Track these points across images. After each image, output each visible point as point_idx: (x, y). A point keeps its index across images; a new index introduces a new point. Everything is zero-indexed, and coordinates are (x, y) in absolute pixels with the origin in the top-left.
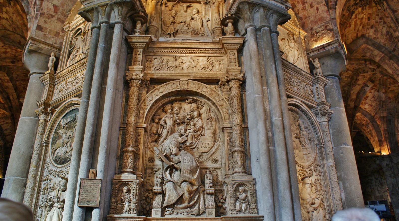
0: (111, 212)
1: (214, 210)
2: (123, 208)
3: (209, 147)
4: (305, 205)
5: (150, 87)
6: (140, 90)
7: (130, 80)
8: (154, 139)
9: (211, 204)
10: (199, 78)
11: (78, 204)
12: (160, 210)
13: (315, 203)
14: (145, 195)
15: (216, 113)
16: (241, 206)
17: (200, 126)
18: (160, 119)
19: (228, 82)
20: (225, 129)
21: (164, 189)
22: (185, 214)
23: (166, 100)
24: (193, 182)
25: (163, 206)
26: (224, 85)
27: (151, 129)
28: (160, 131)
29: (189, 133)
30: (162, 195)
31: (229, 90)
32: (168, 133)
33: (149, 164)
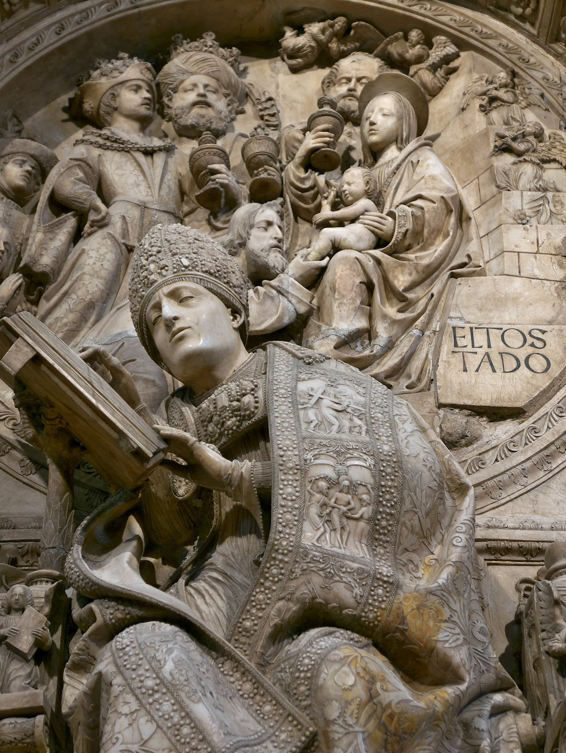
3: (537, 363)
28: (43, 246)
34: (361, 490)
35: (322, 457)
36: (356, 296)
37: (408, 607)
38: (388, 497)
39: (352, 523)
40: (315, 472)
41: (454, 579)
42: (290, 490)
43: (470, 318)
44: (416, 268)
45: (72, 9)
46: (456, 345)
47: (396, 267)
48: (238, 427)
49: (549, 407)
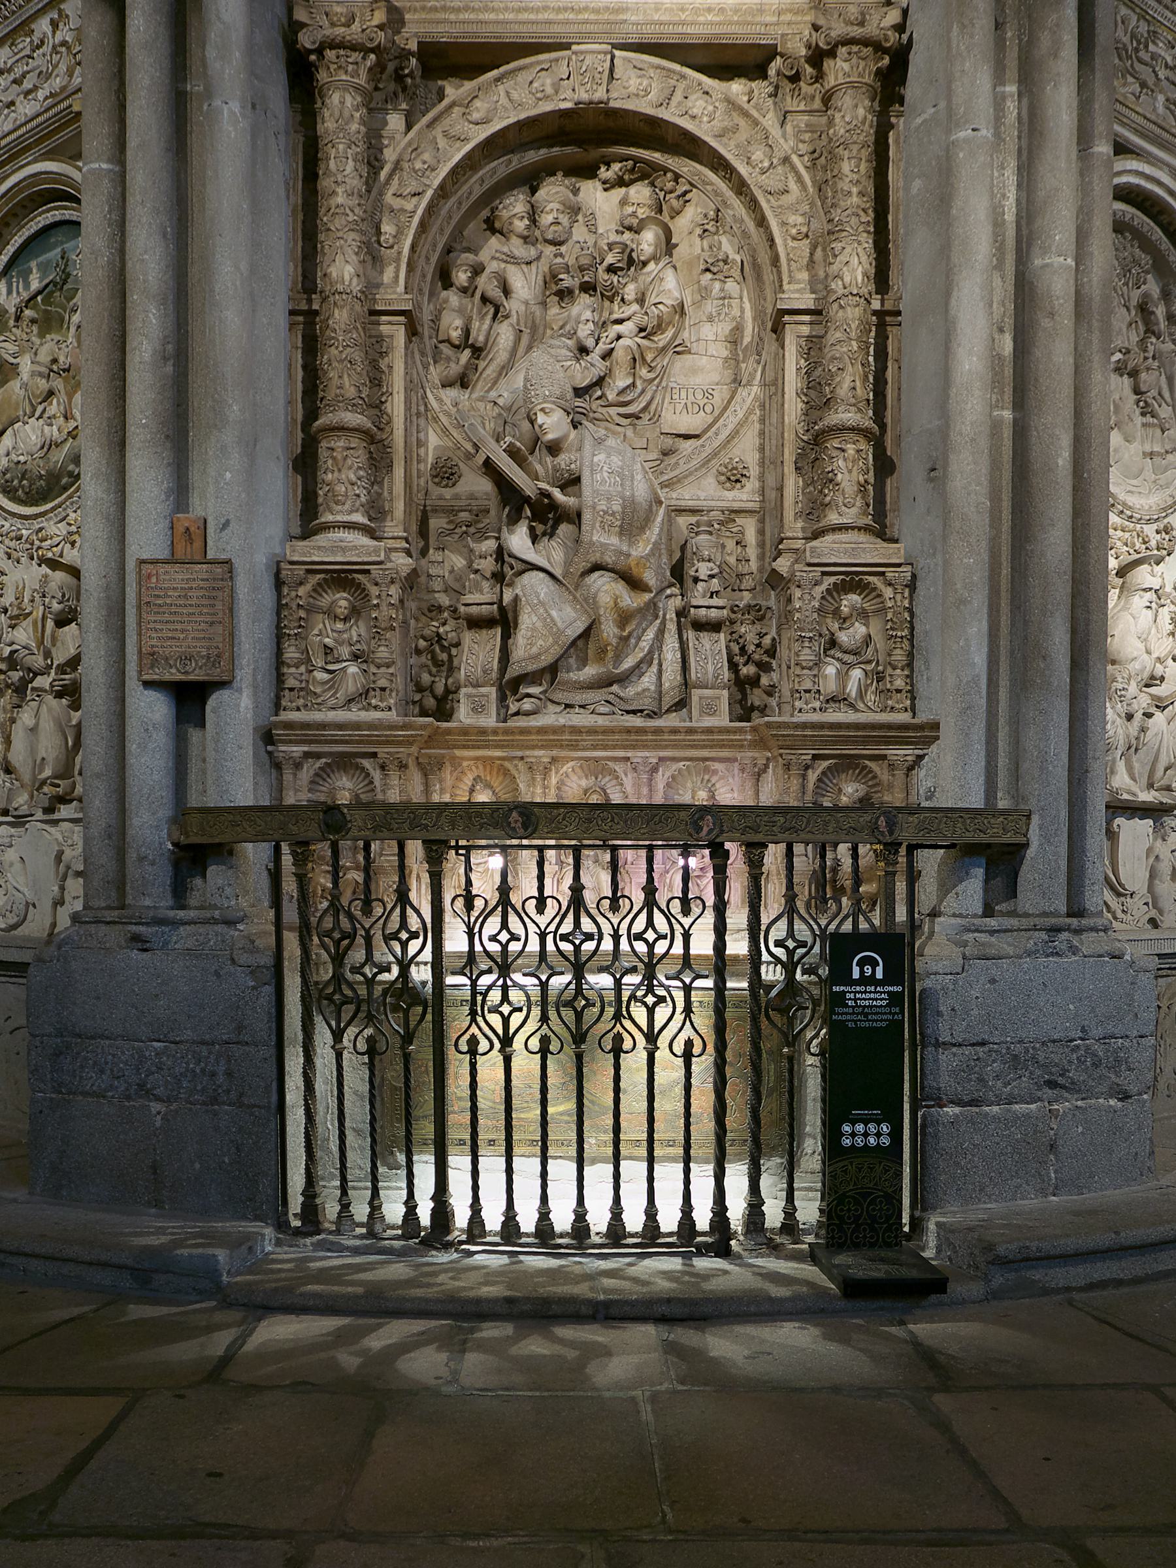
0: (284, 703)
1: (725, 693)
2: (333, 684)
3: (708, 409)
4: (1120, 686)
5: (421, 92)
6: (370, 110)
7: (320, 51)
8: (455, 369)
9: (710, 668)
10: (670, 34)
11: (140, 672)
12: (494, 695)
13: (1162, 679)
14: (427, 632)
15: (745, 234)
16: (843, 677)
17: (669, 302)
18: (477, 270)
19: (818, 57)
20: (787, 318)
21: (508, 597)
22: (602, 709)
23: (500, 167)
24: (635, 571)
25: (507, 677)
26: (795, 79)
27: (436, 320)
28: (479, 330)
29: (619, 337)
30: (498, 631)
31: (817, 104)
32: (518, 340)
33: (436, 491)
37: (633, 564)
40: (598, 508)
41: (652, 550)
45: (487, 168)
49: (709, 434)
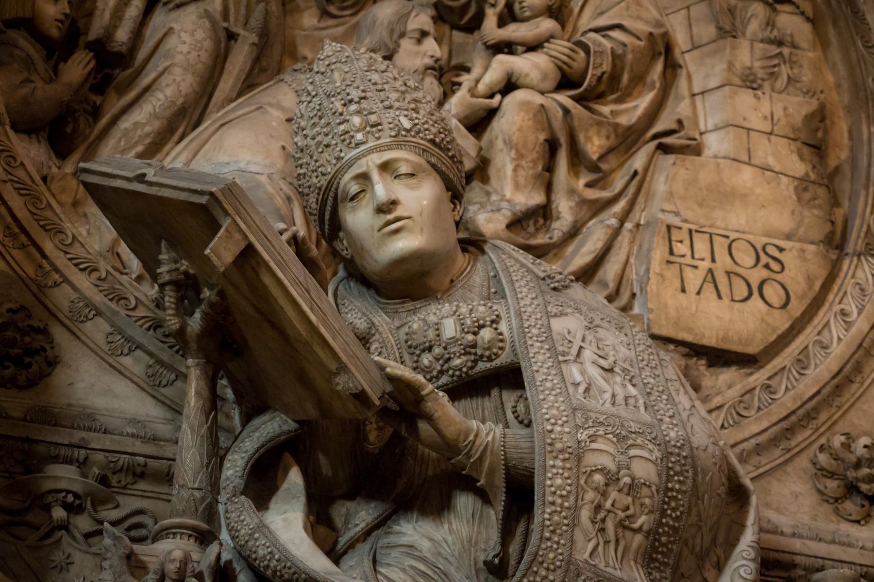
3: (773, 293)
29: (509, 86)
34: (645, 491)
35: (599, 439)
36: (538, 159)
38: (673, 504)
39: (628, 534)
40: (592, 460)
42: (559, 481)
43: (688, 214)
44: (615, 131)
46: (671, 253)
47: (591, 125)
48: (472, 368)
